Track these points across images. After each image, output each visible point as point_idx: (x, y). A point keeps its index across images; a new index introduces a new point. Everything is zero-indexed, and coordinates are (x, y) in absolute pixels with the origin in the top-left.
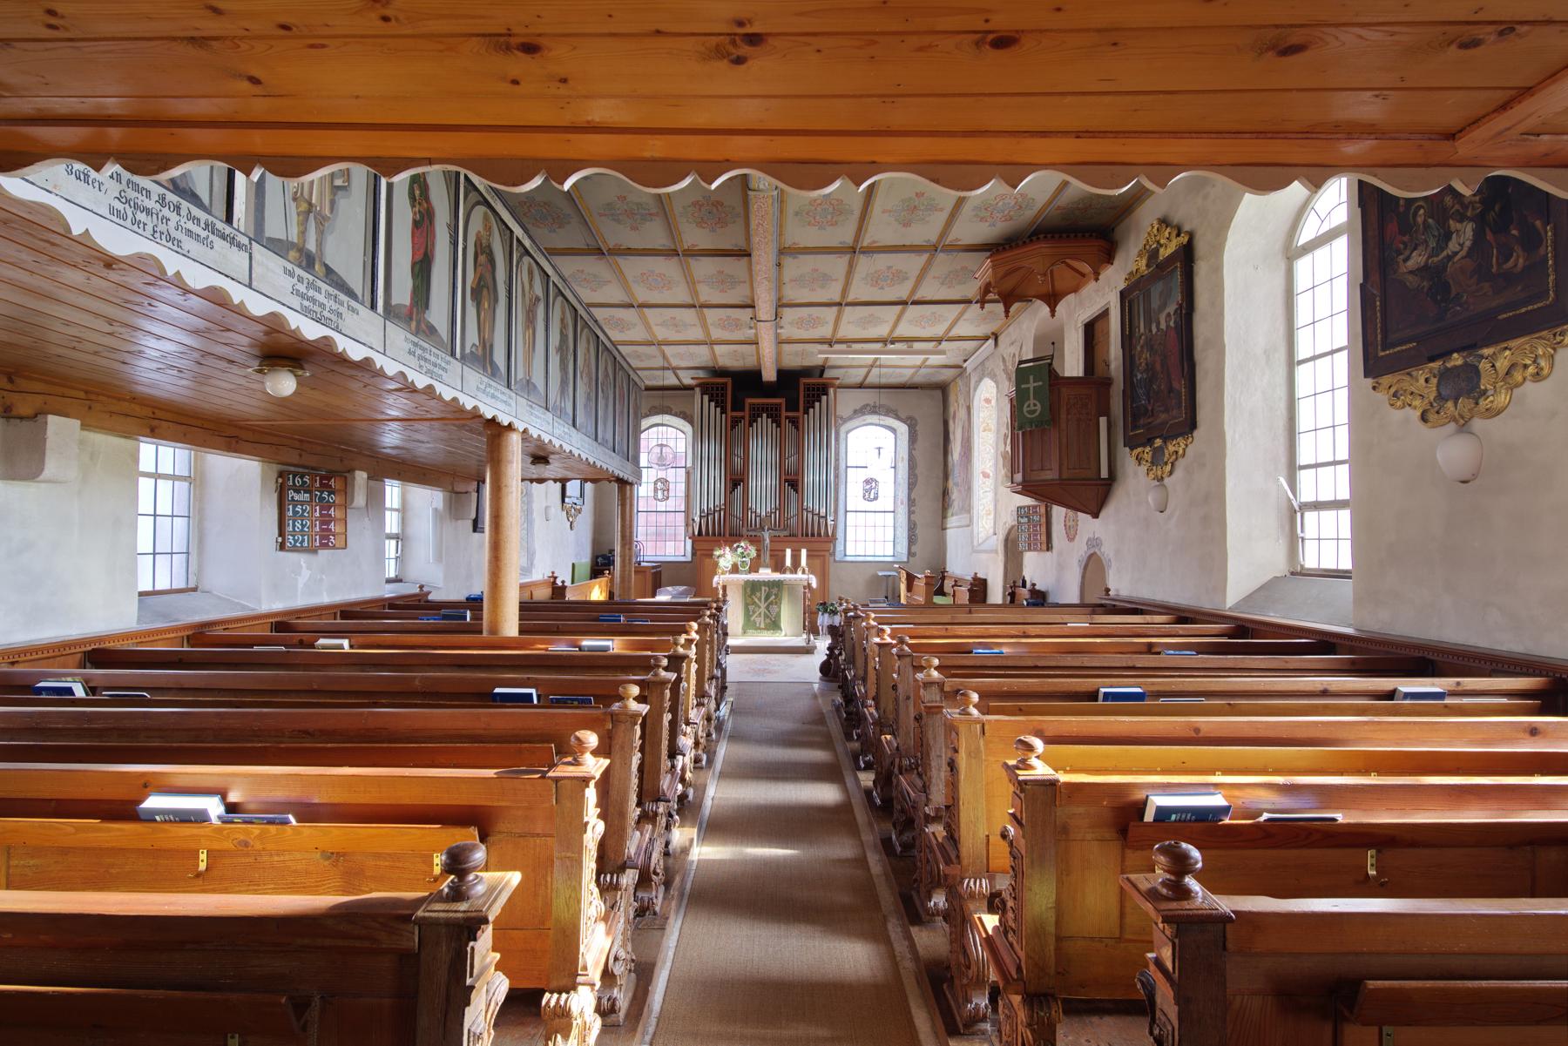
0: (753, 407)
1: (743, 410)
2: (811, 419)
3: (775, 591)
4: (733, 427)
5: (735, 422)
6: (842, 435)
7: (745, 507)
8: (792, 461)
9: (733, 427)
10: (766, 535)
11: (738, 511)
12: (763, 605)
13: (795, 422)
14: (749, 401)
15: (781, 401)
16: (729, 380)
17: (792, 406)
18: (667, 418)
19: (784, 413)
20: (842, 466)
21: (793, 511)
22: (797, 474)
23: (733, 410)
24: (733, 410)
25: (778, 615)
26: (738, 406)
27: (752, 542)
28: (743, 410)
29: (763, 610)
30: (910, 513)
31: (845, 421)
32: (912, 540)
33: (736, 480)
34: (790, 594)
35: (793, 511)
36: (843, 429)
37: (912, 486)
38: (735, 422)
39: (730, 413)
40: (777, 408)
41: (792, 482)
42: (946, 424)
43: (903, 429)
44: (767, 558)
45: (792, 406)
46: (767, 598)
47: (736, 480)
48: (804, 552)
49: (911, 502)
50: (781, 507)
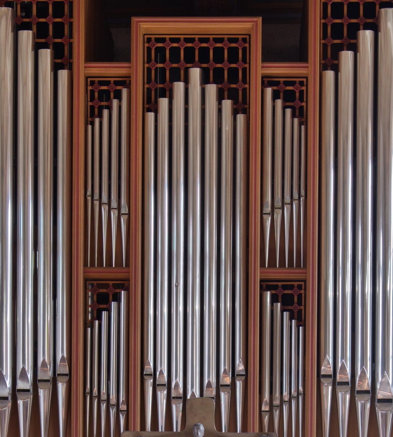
0: (158, 49)
1: (125, 56)
4: (93, 113)
7: (137, 371)
8: (281, 221)
9: (93, 113)
11: (112, 387)
13: (293, 96)
14: (146, 26)
19: (259, 69)
21: (290, 385)
22: (301, 262)
28: (125, 56)
33: (105, 285)
35: (290, 385)
39: (84, 68)
41: (286, 288)
47: (105, 285)
50: (256, 364)
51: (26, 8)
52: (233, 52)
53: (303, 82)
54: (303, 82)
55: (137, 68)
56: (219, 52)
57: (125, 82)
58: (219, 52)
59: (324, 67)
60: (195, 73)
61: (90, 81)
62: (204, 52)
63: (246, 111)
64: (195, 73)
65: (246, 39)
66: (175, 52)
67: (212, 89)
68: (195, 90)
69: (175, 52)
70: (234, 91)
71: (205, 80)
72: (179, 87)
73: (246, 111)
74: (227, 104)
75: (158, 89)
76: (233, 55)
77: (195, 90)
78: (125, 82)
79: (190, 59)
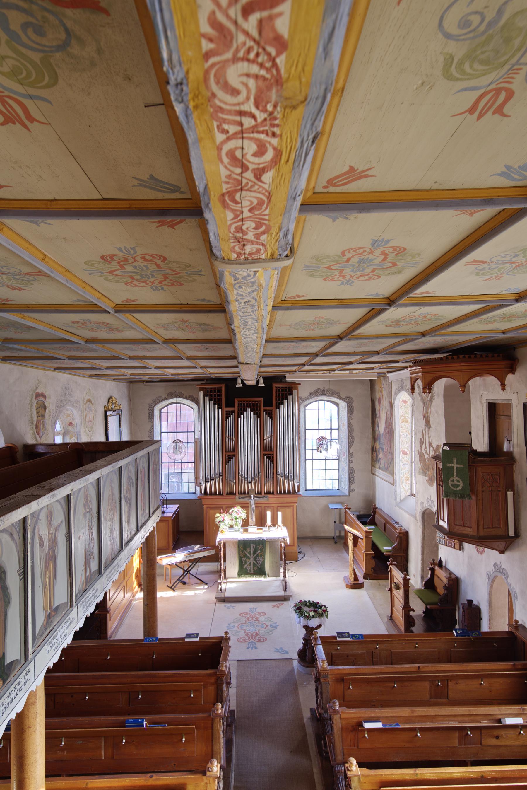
2: (282, 411)
3: (260, 547)
4: (227, 418)
5: (227, 415)
6: (302, 410)
8: (268, 440)
10: (252, 502)
12: (252, 557)
15: (261, 400)
16: (223, 386)
17: (268, 403)
18: (179, 400)
19: (262, 408)
20: (302, 430)
23: (226, 407)
24: (226, 406)
25: (263, 564)
26: (230, 403)
27: (243, 508)
28: (234, 406)
29: (252, 560)
30: (350, 462)
31: (304, 400)
32: (351, 481)
34: (270, 547)
36: (302, 406)
37: (350, 444)
38: (227, 415)
40: (258, 404)
42: (373, 402)
43: (343, 405)
44: (253, 520)
45: (268, 403)
46: (255, 552)
48: (280, 514)
49: (350, 455)
51: (211, 395)
52: (257, 404)
53: (272, 411)
54: (272, 411)
55: (236, 408)
56: (254, 404)
57: (234, 411)
58: (254, 404)
59: (277, 408)
60: (249, 410)
61: (226, 411)
62: (250, 404)
63: (260, 418)
64: (249, 410)
65: (259, 401)
66: (244, 404)
67: (252, 413)
68: (248, 413)
69: (244, 404)
70: (257, 413)
71: (251, 411)
72: (245, 413)
73: (260, 418)
74: (256, 416)
75: (241, 413)
76: (257, 405)
77: (248, 413)
78: (234, 411)
79: (247, 406)
